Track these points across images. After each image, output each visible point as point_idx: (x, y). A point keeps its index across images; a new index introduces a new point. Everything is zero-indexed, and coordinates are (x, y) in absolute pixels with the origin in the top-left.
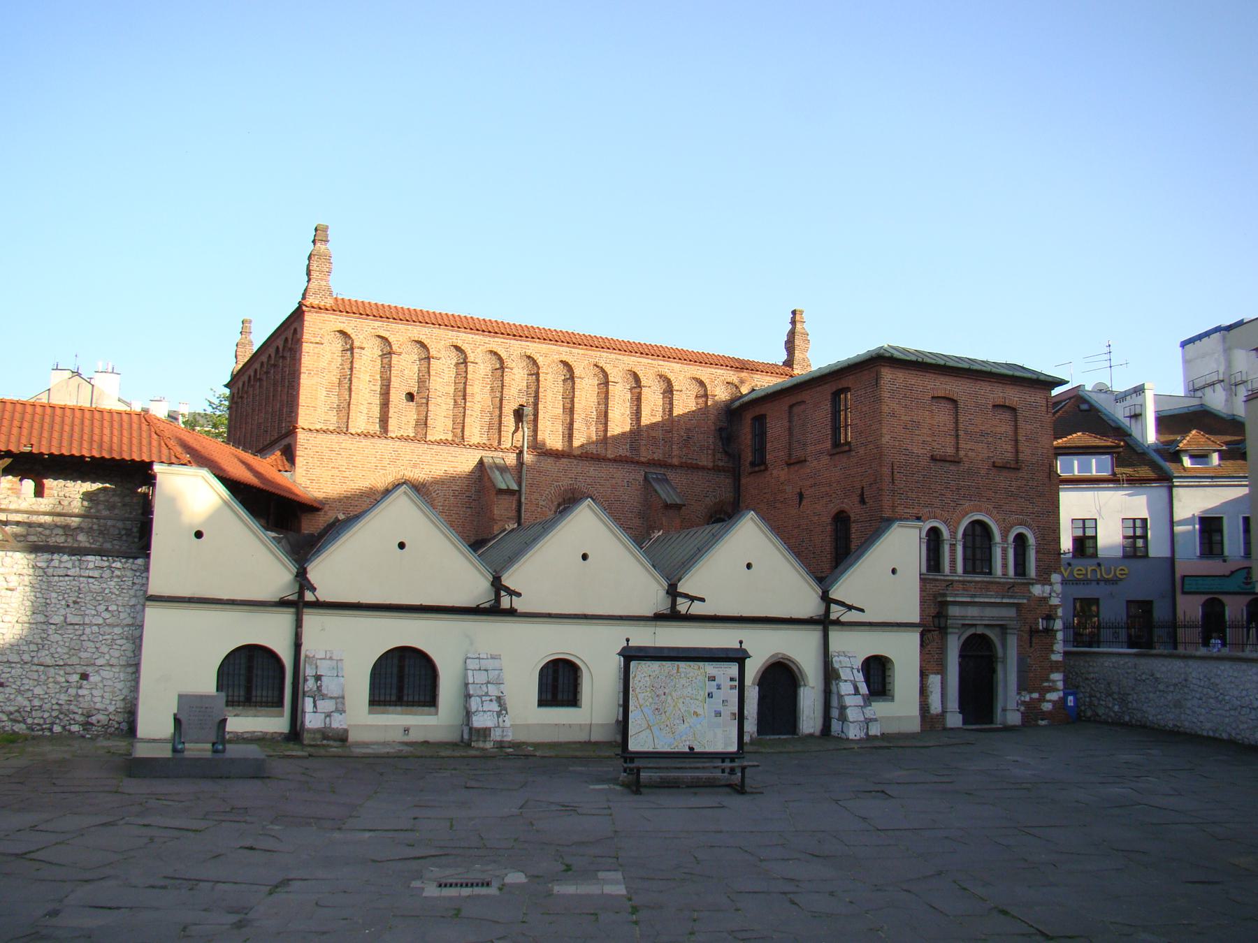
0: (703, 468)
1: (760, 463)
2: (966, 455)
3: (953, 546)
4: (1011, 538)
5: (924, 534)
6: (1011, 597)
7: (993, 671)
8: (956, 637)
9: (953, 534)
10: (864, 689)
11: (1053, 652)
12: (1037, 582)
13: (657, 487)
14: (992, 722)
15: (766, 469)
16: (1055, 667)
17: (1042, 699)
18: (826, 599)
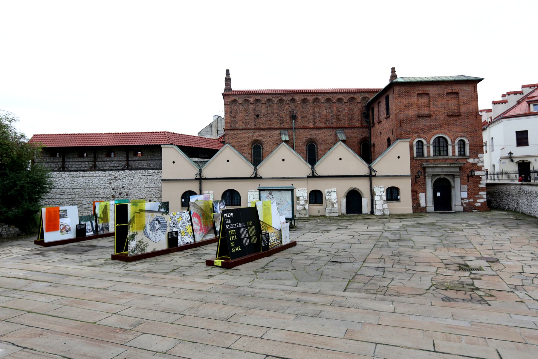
0: (357, 127)
1: (373, 123)
2: (434, 113)
3: (428, 147)
4: (456, 142)
5: (414, 143)
6: (459, 164)
7: (451, 191)
8: (430, 180)
9: (428, 143)
10: (385, 198)
11: (480, 184)
12: (470, 157)
13: (338, 135)
14: (451, 210)
15: (374, 125)
16: (482, 189)
17: (475, 202)
18: (371, 169)
